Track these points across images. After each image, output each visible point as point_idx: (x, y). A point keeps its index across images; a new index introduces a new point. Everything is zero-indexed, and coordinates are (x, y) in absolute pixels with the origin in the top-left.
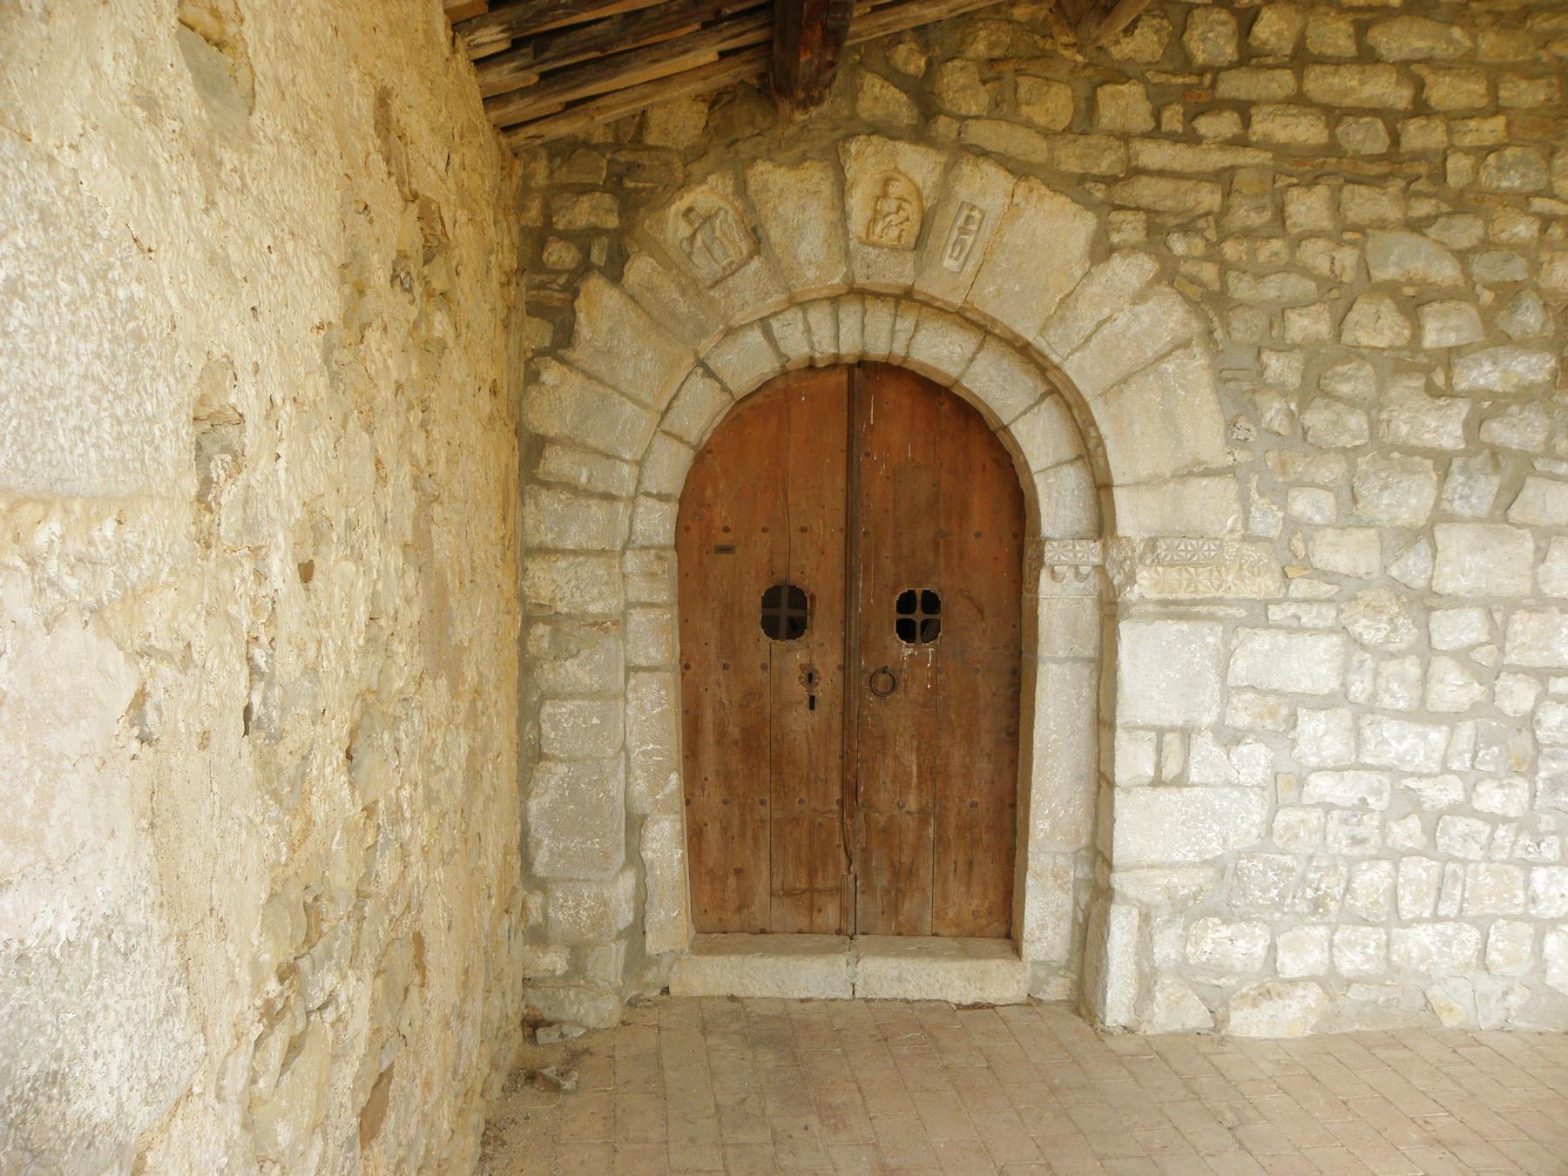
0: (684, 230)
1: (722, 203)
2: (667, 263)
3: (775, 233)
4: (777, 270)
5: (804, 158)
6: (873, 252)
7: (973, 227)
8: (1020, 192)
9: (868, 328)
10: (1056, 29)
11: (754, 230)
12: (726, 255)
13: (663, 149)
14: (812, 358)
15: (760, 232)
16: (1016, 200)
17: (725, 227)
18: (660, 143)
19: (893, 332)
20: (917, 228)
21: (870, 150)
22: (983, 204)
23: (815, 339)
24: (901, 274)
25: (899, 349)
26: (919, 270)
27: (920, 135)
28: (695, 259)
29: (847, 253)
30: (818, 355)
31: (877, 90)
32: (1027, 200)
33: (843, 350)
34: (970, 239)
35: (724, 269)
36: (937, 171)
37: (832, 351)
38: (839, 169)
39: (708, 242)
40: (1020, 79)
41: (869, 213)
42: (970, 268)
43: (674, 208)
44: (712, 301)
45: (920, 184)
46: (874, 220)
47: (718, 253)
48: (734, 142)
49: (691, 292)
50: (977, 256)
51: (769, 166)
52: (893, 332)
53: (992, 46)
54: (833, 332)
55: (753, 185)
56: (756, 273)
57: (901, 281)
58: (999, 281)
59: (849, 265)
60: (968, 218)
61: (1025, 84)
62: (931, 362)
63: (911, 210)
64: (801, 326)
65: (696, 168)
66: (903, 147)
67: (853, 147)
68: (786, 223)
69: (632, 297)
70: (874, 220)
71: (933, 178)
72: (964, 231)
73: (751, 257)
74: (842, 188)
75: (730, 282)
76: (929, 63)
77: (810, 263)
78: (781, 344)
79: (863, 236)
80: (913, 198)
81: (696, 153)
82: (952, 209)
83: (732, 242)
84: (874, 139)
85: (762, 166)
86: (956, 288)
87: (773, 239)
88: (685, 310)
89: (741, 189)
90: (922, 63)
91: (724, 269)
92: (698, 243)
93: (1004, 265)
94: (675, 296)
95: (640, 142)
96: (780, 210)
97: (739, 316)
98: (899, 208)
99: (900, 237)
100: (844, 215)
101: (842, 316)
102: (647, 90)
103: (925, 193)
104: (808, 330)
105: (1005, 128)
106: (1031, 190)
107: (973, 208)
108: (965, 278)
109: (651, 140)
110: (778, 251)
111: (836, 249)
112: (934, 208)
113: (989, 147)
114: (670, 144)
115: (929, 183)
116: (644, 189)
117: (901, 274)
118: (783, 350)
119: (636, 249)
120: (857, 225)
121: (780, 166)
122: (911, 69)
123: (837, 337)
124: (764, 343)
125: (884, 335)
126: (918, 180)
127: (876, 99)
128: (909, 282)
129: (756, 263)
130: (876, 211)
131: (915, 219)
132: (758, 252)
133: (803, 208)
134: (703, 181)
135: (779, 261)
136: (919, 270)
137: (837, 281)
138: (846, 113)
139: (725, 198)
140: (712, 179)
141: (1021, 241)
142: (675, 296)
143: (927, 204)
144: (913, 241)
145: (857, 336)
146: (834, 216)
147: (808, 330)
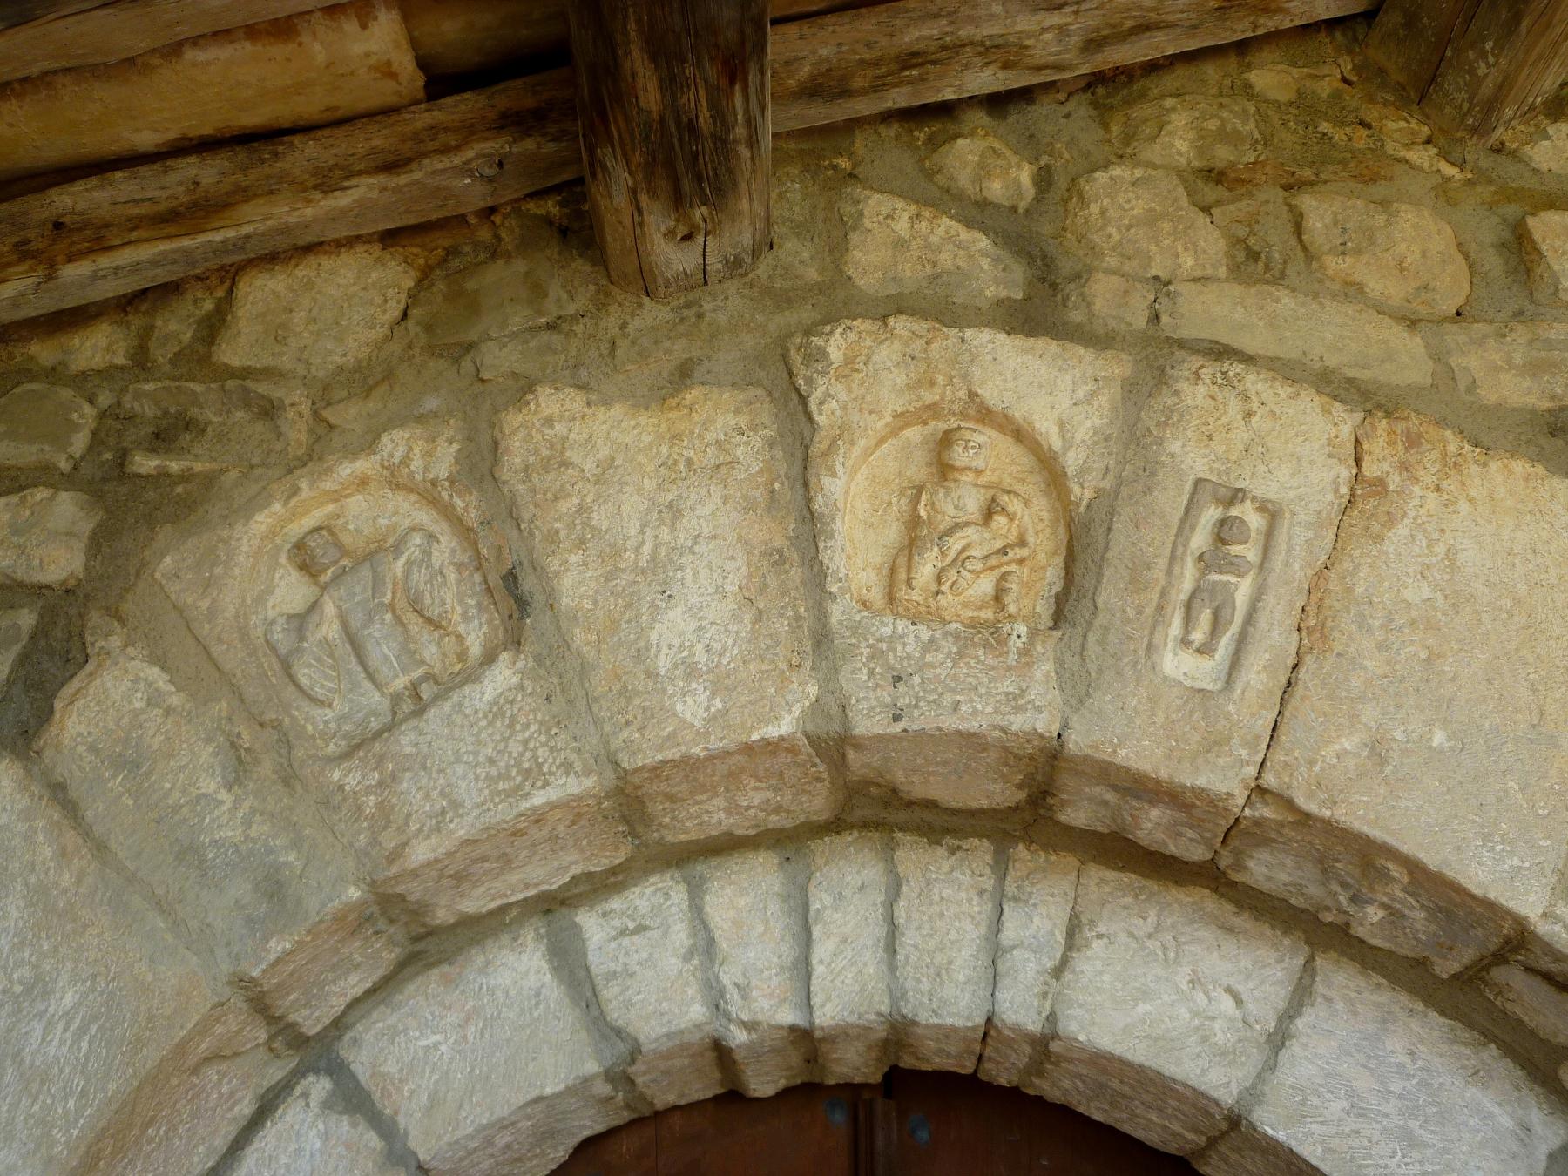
0: (291, 591)
1: (425, 516)
2: (200, 670)
3: (575, 583)
4: (564, 681)
5: (684, 374)
6: (914, 636)
7: (1249, 552)
8: (1376, 446)
9: (909, 939)
10: (1372, 114)
11: (511, 579)
12: (409, 654)
13: (267, 373)
14: (721, 1052)
15: (528, 583)
16: (1370, 469)
17: (419, 577)
18: (264, 360)
19: (995, 952)
20: (1053, 575)
21: (886, 354)
22: (1270, 483)
23: (728, 977)
24: (1015, 701)
25: (1020, 1009)
26: (1078, 688)
27: (1041, 310)
28: (303, 675)
29: (822, 638)
30: (738, 1037)
31: (902, 225)
32: (1404, 467)
33: (827, 1014)
34: (1243, 591)
35: (396, 699)
36: (1103, 400)
37: (788, 1016)
38: (794, 406)
39: (355, 622)
40: (1307, 202)
41: (892, 533)
42: (1258, 676)
43: (262, 521)
44: (330, 801)
45: (1057, 444)
46: (911, 545)
47: (383, 648)
48: (470, 347)
49: (266, 768)
50: (1276, 638)
51: (574, 401)
52: (995, 952)
53: (1203, 142)
54: (788, 951)
55: (517, 453)
56: (496, 711)
57: (1018, 723)
58: (1369, 714)
59: (828, 681)
60: (1224, 532)
61: (1319, 212)
62: (1137, 1052)
63: (1032, 516)
64: (680, 935)
65: (349, 415)
66: (983, 339)
67: (836, 346)
68: (616, 552)
69: (58, 792)
70: (911, 545)
71: (1090, 422)
72: (1217, 558)
73: (489, 658)
74: (801, 449)
75: (406, 741)
76: (1044, 180)
77: (692, 672)
78: (610, 993)
79: (876, 596)
80: (1033, 488)
81: (366, 379)
82: (1170, 501)
83: (434, 624)
84: (900, 324)
85: (547, 401)
86: (1215, 744)
87: (566, 601)
88: (232, 833)
89: (482, 464)
90: (1025, 176)
91: (396, 699)
92: (328, 628)
93: (1374, 664)
94: (209, 785)
95: (205, 360)
96: (599, 518)
97: (420, 853)
98: (989, 512)
99: (998, 597)
100: (810, 527)
101: (820, 899)
102: (207, 173)
103: (1072, 461)
104: (705, 947)
105: (1286, 302)
106: (1412, 441)
107: (1236, 496)
108: (1250, 707)
109: (233, 352)
110: (579, 637)
111: (782, 626)
112: (1107, 502)
113: (1250, 345)
114: (286, 361)
115: (1083, 432)
116: (186, 477)
117: (1015, 701)
118: (615, 1014)
119: (115, 642)
120: (858, 548)
121: (607, 403)
122: (996, 189)
123: (802, 969)
124: (554, 992)
125: (965, 959)
126: (1047, 428)
127: (901, 244)
128: (1046, 724)
129: (502, 676)
130: (914, 522)
131: (1045, 544)
132: (515, 641)
133: (675, 511)
134: (369, 445)
135: (584, 671)
136: (1078, 688)
137: (784, 726)
138: (812, 274)
139: (429, 495)
140: (394, 444)
141: (1417, 592)
142: (209, 785)
143: (1082, 492)
144: (1045, 610)
145: (871, 963)
146: (777, 533)
147: (705, 947)
